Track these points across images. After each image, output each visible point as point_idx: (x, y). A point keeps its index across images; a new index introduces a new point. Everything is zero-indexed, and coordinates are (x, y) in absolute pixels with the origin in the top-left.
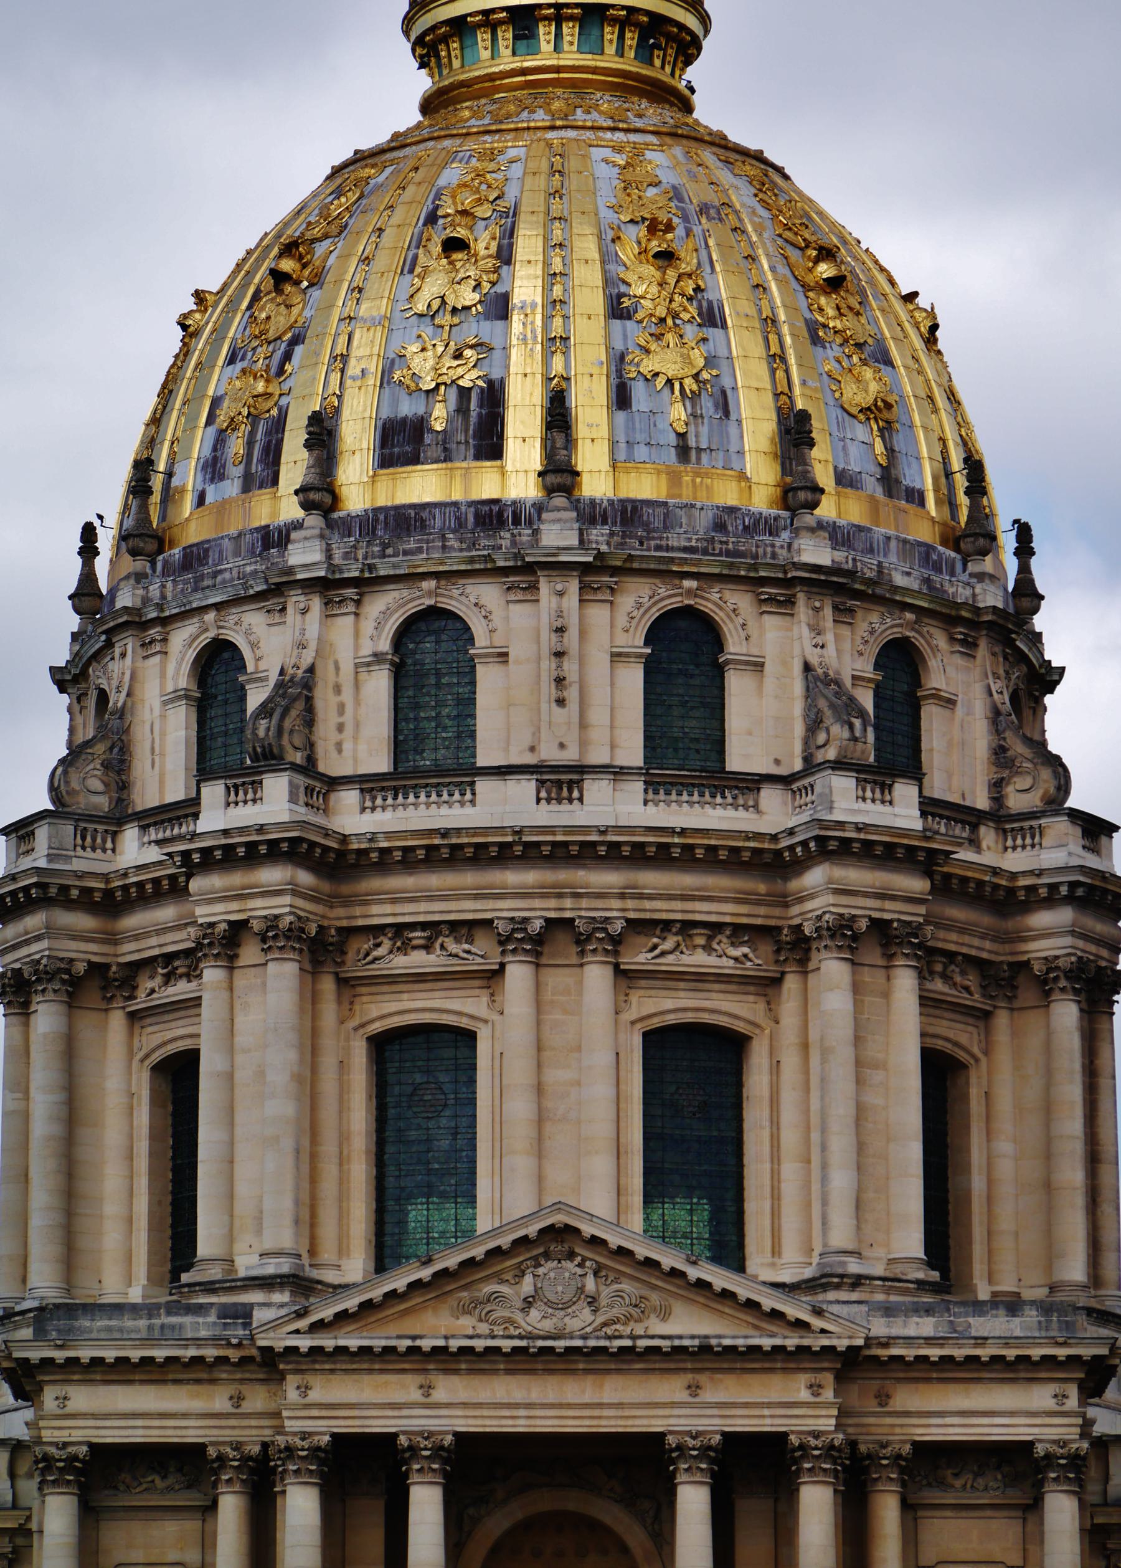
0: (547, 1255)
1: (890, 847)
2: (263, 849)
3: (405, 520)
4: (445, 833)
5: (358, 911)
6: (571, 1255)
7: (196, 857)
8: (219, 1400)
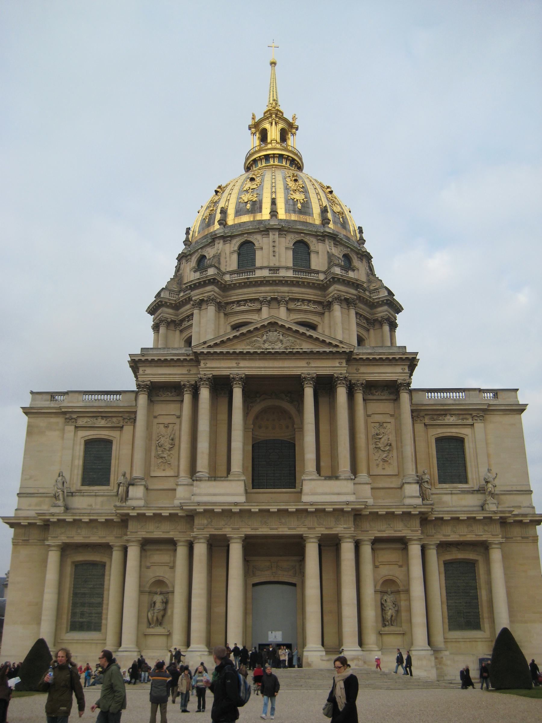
0: (270, 331)
1: (349, 282)
2: (207, 282)
3: (240, 225)
4: (248, 278)
5: (229, 298)
6: (276, 331)
7: (193, 286)
8: (184, 371)
